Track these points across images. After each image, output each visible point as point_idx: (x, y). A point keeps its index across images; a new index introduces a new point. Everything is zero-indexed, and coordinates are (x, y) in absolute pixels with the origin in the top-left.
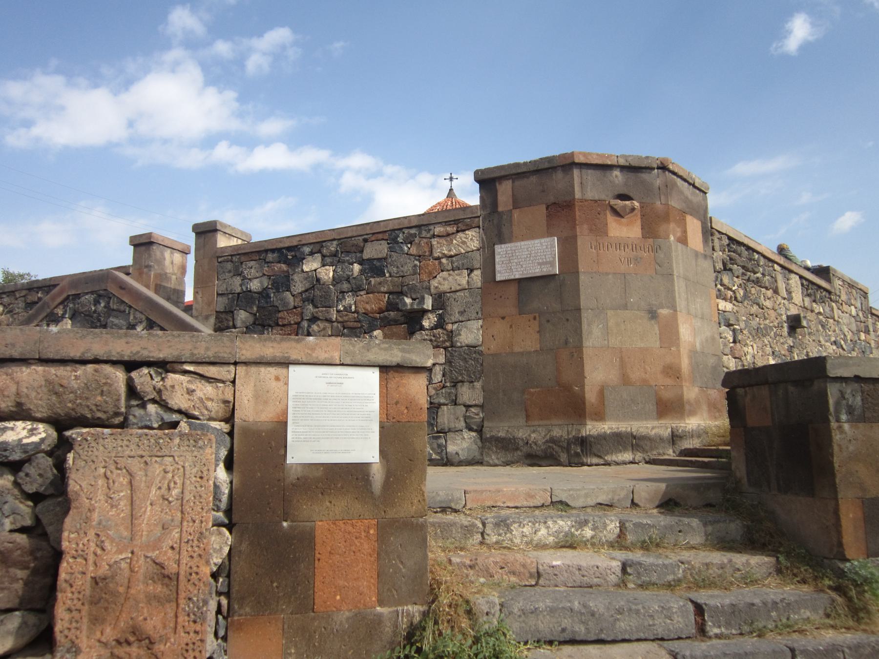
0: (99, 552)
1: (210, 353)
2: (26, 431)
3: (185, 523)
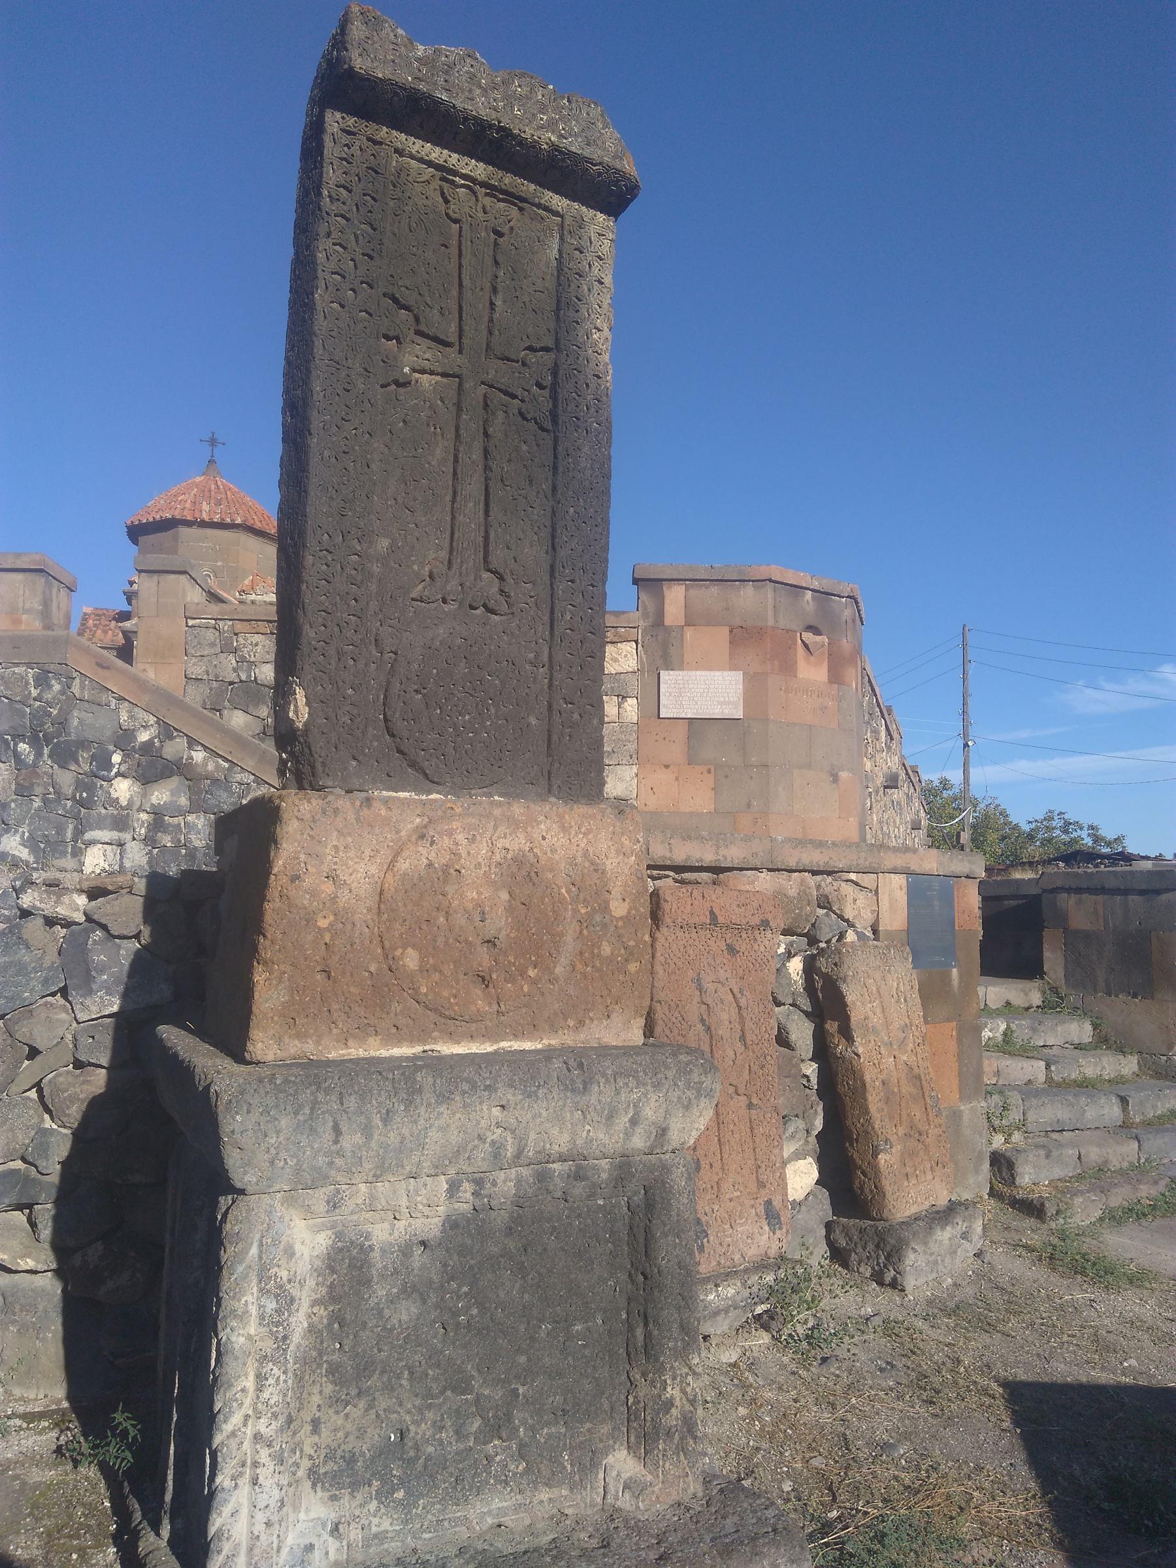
1: (867, 864)
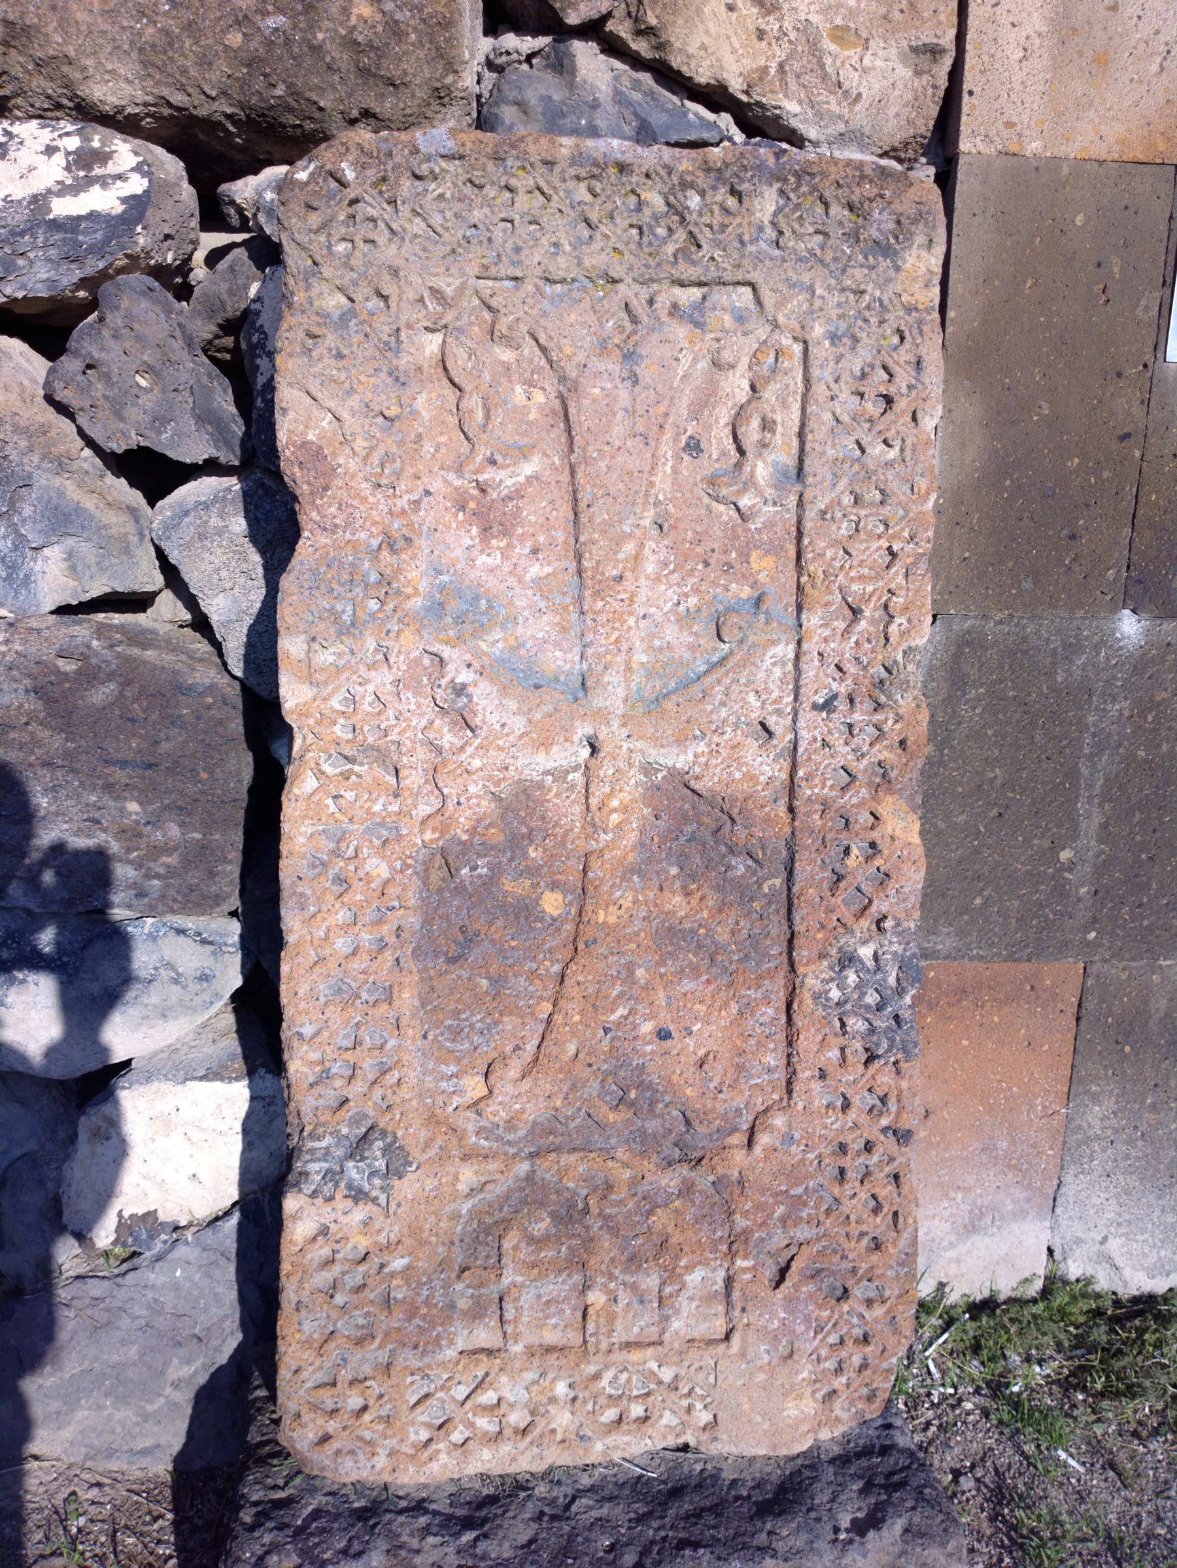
0: (448, 739)
2: (59, 159)
3: (812, 620)
